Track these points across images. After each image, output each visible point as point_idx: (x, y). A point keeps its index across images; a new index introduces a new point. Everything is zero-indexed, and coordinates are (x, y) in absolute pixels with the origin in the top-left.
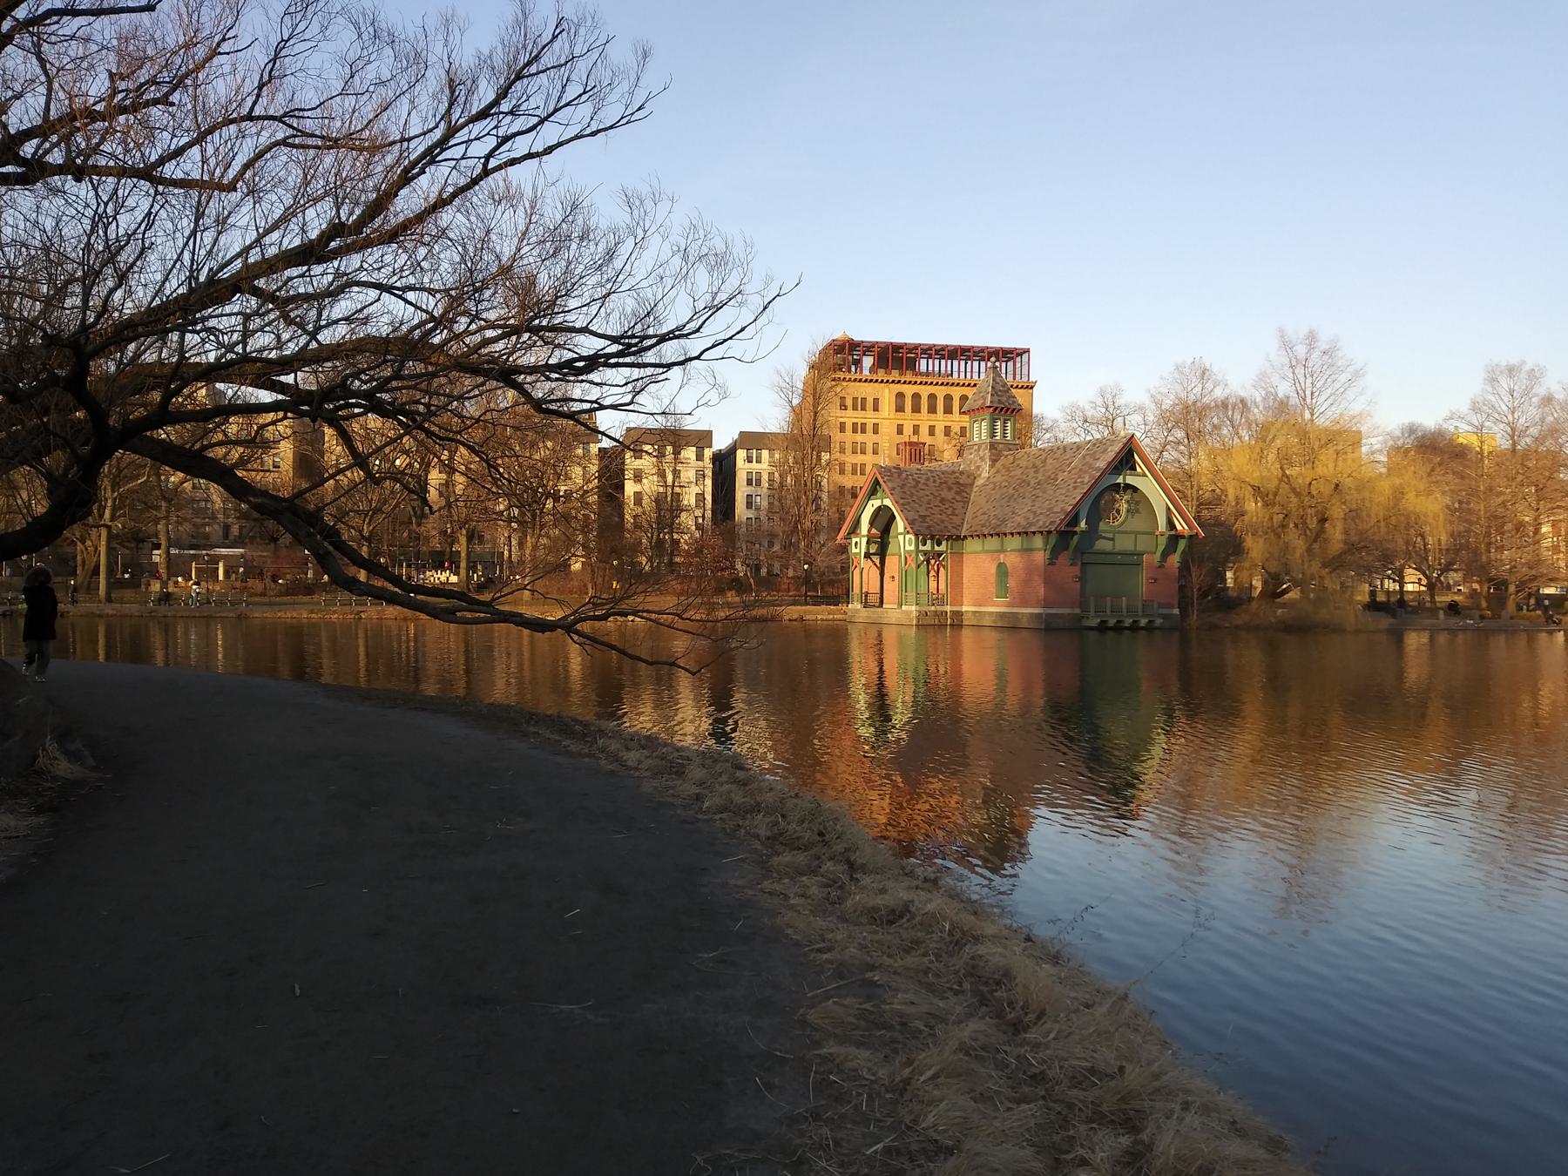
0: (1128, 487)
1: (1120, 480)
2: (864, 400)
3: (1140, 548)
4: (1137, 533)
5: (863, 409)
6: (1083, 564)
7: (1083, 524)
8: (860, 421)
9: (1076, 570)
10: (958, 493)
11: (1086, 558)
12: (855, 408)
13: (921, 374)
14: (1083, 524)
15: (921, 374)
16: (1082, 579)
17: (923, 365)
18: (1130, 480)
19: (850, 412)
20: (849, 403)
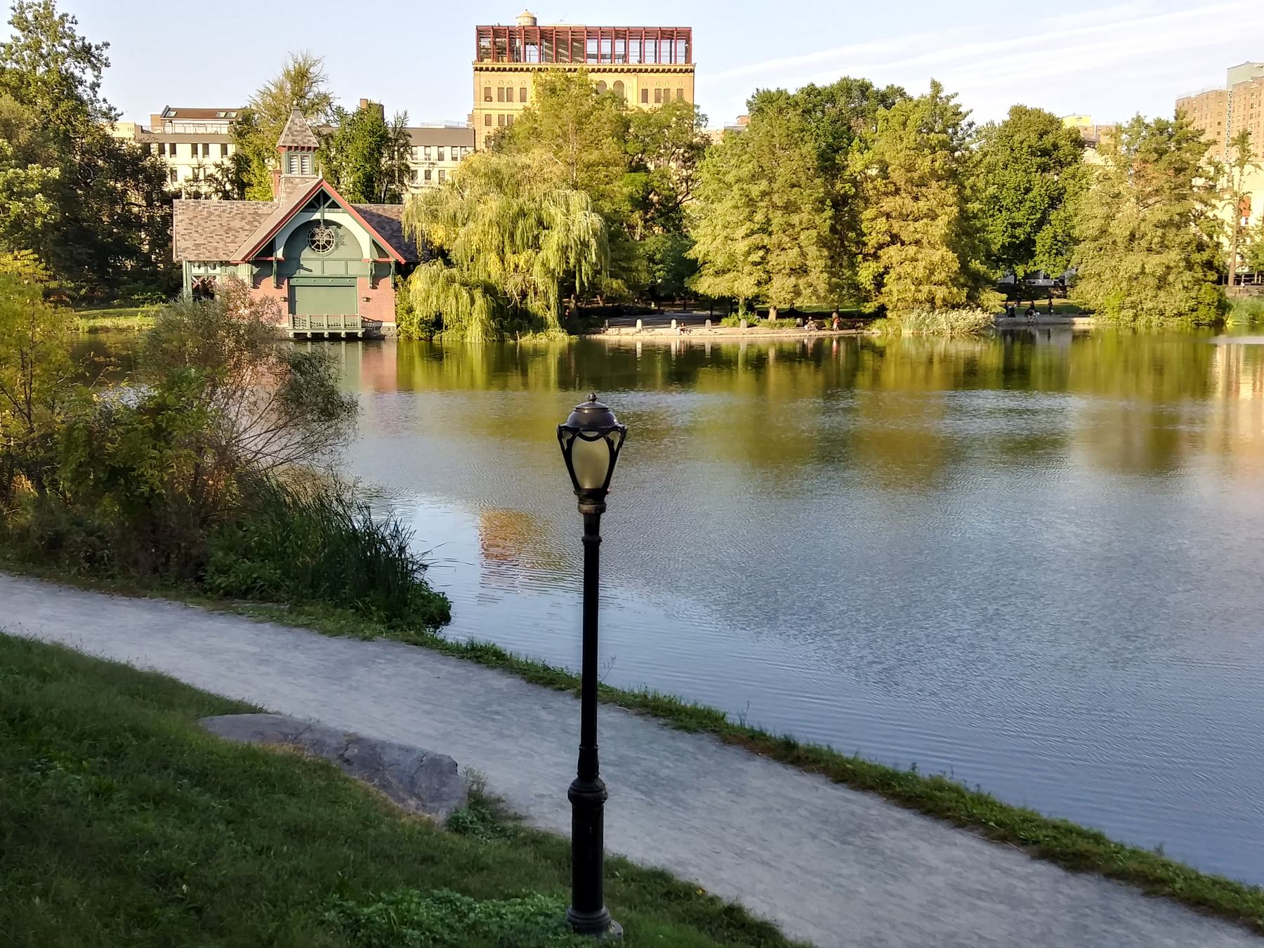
0: (328, 223)
1: (317, 216)
2: (510, 89)
3: (351, 273)
4: (347, 260)
5: (510, 99)
6: (292, 289)
7: (279, 254)
8: (506, 113)
9: (284, 292)
10: (249, 223)
11: (293, 282)
12: (500, 99)
13: (593, 56)
14: (279, 254)
15: (593, 56)
16: (291, 300)
17: (591, 47)
18: (330, 216)
19: (495, 104)
20: (494, 94)
